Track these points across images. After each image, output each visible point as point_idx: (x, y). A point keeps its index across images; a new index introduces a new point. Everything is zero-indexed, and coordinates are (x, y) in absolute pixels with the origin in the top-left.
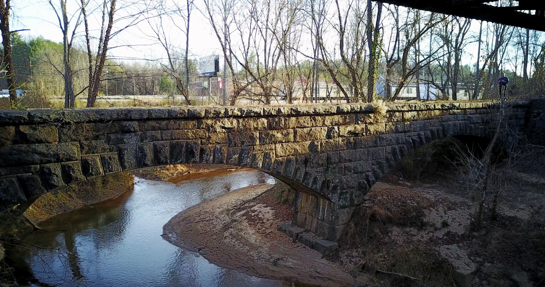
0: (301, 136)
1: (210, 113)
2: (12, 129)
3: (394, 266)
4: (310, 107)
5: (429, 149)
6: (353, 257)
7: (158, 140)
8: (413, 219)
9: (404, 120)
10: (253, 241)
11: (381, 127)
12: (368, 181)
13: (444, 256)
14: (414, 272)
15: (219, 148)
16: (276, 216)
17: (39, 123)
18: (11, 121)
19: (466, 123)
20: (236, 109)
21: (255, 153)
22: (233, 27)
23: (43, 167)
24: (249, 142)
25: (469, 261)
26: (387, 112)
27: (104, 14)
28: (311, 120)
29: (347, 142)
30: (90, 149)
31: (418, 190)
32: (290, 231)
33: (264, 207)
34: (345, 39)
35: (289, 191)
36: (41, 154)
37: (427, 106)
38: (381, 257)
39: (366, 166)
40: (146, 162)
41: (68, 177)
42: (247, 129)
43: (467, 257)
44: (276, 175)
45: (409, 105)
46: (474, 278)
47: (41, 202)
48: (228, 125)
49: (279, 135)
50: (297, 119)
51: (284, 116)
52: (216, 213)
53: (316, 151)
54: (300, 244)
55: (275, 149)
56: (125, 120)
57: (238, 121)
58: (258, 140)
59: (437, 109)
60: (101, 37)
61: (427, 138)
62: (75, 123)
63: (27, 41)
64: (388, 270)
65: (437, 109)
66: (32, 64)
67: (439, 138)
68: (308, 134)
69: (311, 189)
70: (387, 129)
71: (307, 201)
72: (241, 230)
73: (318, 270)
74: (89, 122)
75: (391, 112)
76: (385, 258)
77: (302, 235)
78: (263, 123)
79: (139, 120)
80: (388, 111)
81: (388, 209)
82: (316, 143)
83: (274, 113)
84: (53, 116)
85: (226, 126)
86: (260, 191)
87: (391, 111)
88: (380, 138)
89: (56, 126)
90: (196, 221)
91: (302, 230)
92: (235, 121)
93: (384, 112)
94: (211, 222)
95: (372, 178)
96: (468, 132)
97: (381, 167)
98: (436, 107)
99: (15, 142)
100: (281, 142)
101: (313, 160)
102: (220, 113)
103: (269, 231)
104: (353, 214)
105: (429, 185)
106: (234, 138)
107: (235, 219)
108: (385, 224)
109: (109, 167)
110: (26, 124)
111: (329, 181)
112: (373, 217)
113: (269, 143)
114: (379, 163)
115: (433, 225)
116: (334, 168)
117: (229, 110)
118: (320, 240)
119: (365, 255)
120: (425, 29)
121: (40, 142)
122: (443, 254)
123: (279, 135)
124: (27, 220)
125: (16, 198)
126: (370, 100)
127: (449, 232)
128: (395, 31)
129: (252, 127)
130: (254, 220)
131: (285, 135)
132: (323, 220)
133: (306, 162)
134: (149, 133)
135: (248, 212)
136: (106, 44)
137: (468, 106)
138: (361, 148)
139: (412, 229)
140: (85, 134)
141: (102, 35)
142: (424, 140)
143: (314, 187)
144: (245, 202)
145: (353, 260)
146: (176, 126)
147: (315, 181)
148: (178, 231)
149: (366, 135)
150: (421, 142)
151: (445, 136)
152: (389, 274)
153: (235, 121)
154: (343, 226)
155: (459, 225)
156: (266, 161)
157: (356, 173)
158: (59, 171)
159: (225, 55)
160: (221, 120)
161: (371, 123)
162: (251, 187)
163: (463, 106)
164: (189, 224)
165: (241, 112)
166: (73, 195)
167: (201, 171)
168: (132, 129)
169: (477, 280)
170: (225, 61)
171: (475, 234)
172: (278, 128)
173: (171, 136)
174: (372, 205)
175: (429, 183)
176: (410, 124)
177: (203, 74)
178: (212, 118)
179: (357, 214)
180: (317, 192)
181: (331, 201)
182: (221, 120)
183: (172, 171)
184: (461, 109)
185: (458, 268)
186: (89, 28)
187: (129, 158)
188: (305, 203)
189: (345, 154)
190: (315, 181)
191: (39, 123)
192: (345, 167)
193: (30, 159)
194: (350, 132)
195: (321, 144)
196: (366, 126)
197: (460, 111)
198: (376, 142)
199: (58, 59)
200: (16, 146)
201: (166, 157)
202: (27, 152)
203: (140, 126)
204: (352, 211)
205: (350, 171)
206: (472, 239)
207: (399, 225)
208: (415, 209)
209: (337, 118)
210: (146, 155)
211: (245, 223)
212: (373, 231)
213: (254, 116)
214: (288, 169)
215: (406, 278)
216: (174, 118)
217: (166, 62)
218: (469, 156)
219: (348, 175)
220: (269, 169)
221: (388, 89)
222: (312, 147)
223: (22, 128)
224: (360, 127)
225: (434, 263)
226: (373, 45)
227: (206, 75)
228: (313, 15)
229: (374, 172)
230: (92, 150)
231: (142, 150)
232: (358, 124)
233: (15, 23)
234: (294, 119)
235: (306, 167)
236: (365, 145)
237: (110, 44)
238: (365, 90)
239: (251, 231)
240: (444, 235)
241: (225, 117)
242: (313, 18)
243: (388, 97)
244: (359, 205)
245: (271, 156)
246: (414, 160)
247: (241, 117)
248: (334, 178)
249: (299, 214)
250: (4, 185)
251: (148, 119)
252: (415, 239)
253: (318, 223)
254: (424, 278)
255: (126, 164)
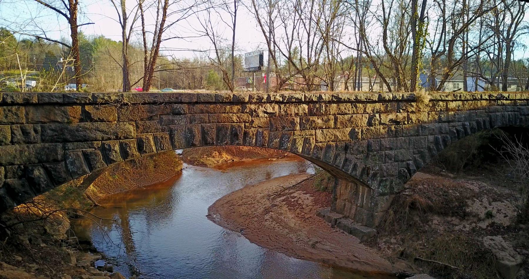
0: (342, 123)
1: (254, 98)
2: (79, 108)
3: (434, 254)
4: (351, 94)
5: (474, 141)
6: (391, 244)
7: (206, 123)
8: (455, 209)
9: (447, 109)
10: (292, 225)
11: (424, 117)
12: (409, 170)
13: (487, 246)
14: (455, 261)
15: (261, 131)
16: (316, 202)
17: (102, 104)
18: (78, 102)
19: (516, 114)
20: (278, 95)
21: (295, 137)
22: (278, 23)
23: (104, 144)
24: (290, 127)
25: (515, 252)
26: (430, 101)
27: (158, 9)
28: (352, 107)
29: (388, 130)
30: (144, 129)
31: (461, 181)
32: (329, 217)
33: (304, 194)
34: (388, 32)
35: (329, 179)
36: (102, 131)
37: (473, 96)
38: (421, 245)
39: (407, 154)
40: (194, 142)
41: (125, 154)
42: (288, 114)
43: (512, 249)
44: (315, 160)
45: (454, 95)
46: (519, 270)
47: (101, 182)
48: (270, 110)
49: (319, 121)
50: (338, 105)
51: (325, 102)
52: (258, 198)
53: (357, 138)
54: (338, 229)
55: (315, 135)
56: (175, 103)
57: (280, 107)
58: (299, 125)
59: (484, 99)
60: (156, 30)
61: (472, 129)
62: (132, 104)
63: (91, 40)
64: (427, 258)
65: (484, 99)
66: (95, 60)
67: (485, 128)
68: (349, 120)
69: (351, 176)
70: (429, 119)
71: (346, 188)
72: (281, 214)
73: (356, 255)
74: (144, 104)
75: (435, 102)
76: (424, 246)
77: (340, 220)
78: (304, 109)
79: (189, 103)
80: (431, 101)
81: (429, 198)
82: (356, 130)
83: (315, 99)
84: (113, 98)
85: (268, 111)
86: (299, 179)
87: (434, 100)
88: (422, 127)
89: (116, 107)
90: (238, 204)
91: (341, 216)
92: (277, 107)
93: (426, 101)
94: (253, 205)
95: (413, 167)
96: (518, 124)
97: (423, 157)
98: (483, 97)
99: (81, 120)
100: (321, 128)
101: (353, 147)
102: (263, 98)
103: (308, 216)
104: (392, 201)
105: (472, 177)
106: (275, 123)
107: (275, 203)
108: (425, 212)
109: (161, 146)
110: (90, 104)
111: (369, 168)
112: (413, 206)
113: (310, 128)
114: (420, 152)
115: (476, 216)
116: (374, 155)
117: (271, 96)
118: (358, 226)
119: (403, 242)
120: (473, 18)
121: (102, 121)
122: (486, 244)
123: (319, 121)
124: (89, 197)
125: (81, 170)
126: (413, 89)
127: (493, 223)
128: (441, 24)
129: (293, 113)
130: (293, 206)
131: (326, 122)
132: (362, 207)
133: (346, 148)
134: (197, 116)
135: (288, 198)
136: (159, 37)
137: (518, 97)
138: (403, 136)
139: (454, 218)
140: (140, 114)
141: (156, 28)
142: (469, 131)
143: (354, 173)
144: (285, 189)
145: (392, 246)
146: (222, 110)
147: (355, 167)
148: (222, 213)
149: (408, 123)
150: (466, 133)
151: (492, 127)
152: (427, 262)
153: (277, 107)
154: (382, 213)
155: (505, 217)
156: (306, 146)
157: (397, 161)
158: (117, 148)
159: (269, 48)
160: (264, 106)
161: (412, 112)
162: (291, 175)
163: (512, 96)
164: (232, 207)
165: (283, 98)
166: (129, 177)
167: (244, 160)
168: (182, 112)
169: (523, 272)
170: (269, 56)
171: (522, 226)
172: (319, 114)
173: (218, 119)
174: (412, 193)
175: (474, 175)
176: (455, 114)
177: (249, 68)
178: (255, 103)
179: (397, 202)
180: (357, 179)
181: (370, 188)
182: (264, 106)
183: (217, 159)
184: (511, 100)
185: (503, 259)
186: (145, 22)
187: (179, 137)
188: (344, 190)
189: (386, 142)
190: (355, 167)
191: (102, 104)
192: (386, 155)
193: (93, 135)
194: (391, 120)
195: (362, 131)
196: (408, 115)
197: (509, 102)
198: (418, 131)
199: (118, 56)
200: (82, 124)
201: (213, 139)
202: (90, 130)
203: (189, 109)
204: (391, 199)
205: (391, 159)
206: (519, 231)
207: (439, 214)
208: (458, 199)
209: (378, 106)
210: (194, 136)
211: (285, 208)
212: (412, 219)
213: (295, 102)
214: (328, 155)
215: (446, 267)
216: (220, 103)
217: (213, 56)
218: (517, 146)
219: (388, 162)
220: (309, 154)
221: (432, 77)
222: (353, 134)
223: (87, 108)
224: (401, 115)
225: (476, 253)
226: (417, 35)
227: (251, 69)
228: (357, 7)
229: (415, 161)
230: (146, 130)
231: (191, 131)
232: (400, 112)
233: (82, 18)
234: (334, 105)
235: (346, 153)
236: (406, 134)
237: (164, 36)
238: (409, 83)
239: (290, 215)
240: (487, 226)
241: (268, 103)
242: (357, 11)
243: (432, 87)
244: (399, 193)
245: (311, 141)
246: (458, 152)
247: (282, 103)
248: (375, 166)
249: (338, 201)
250: (72, 159)
251: (197, 103)
252: (457, 228)
253: (356, 210)
254: (465, 268)
255: (176, 144)
